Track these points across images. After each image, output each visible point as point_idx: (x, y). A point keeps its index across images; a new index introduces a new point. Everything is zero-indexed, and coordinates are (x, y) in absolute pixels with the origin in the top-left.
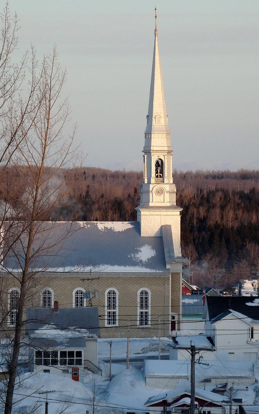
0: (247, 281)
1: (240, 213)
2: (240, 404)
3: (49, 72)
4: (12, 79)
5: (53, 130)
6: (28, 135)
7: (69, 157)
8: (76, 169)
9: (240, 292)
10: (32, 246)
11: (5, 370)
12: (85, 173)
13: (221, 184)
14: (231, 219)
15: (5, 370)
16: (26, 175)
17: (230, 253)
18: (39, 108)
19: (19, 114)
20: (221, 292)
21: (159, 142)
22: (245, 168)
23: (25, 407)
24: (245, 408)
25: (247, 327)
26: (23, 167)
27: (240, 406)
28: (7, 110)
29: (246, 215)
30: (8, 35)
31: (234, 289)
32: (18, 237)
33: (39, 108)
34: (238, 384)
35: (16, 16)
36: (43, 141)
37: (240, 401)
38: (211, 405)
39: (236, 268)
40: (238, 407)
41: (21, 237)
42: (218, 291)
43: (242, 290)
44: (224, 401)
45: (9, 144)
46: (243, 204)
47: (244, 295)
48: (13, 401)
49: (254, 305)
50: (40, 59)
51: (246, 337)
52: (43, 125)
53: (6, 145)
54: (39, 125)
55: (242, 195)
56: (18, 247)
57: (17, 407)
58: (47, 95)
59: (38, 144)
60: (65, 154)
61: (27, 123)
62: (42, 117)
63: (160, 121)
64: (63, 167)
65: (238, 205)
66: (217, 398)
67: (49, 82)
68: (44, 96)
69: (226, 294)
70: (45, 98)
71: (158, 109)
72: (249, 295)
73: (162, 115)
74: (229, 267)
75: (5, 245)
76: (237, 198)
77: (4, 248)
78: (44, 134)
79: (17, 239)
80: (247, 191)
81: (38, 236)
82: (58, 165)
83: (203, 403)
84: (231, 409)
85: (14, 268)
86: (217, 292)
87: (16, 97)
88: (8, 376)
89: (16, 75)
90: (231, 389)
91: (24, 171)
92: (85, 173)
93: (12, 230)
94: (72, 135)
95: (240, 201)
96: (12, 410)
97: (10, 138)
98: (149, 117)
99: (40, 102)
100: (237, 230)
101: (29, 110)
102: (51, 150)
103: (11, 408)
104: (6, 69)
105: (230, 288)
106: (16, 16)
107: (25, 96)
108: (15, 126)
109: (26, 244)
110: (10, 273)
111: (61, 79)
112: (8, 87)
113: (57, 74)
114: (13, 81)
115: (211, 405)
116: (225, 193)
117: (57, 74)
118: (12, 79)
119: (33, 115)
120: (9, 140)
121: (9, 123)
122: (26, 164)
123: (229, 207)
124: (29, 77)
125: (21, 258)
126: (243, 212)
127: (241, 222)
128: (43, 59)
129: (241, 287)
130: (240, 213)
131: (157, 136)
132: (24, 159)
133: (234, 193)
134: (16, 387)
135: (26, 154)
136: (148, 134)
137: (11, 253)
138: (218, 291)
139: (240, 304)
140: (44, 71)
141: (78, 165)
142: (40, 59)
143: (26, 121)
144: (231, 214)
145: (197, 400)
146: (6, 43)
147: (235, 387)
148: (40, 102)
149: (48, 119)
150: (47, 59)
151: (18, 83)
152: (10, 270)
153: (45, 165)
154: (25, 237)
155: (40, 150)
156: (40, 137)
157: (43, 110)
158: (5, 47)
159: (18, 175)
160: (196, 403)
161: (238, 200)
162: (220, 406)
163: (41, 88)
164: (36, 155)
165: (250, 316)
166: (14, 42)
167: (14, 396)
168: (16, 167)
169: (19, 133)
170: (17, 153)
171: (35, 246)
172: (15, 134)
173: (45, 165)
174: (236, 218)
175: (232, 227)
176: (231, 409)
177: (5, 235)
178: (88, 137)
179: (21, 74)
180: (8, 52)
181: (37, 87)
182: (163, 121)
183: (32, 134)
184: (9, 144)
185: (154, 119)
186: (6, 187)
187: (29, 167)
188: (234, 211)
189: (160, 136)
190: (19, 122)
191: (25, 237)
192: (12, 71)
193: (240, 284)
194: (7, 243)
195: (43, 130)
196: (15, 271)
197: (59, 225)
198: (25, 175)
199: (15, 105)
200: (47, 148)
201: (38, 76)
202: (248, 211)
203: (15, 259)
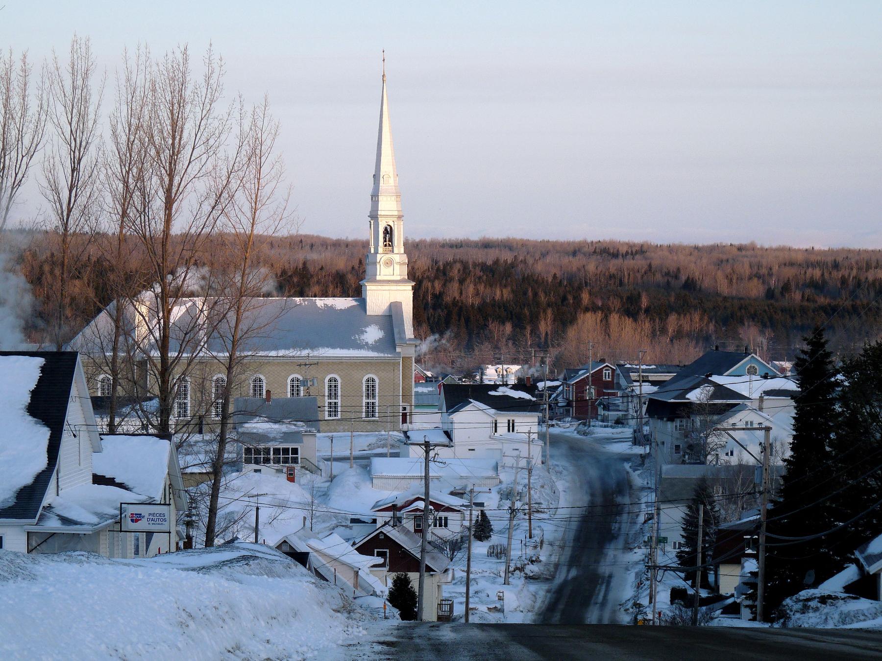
0: (490, 366)
1: (481, 288)
2: (482, 508)
3: (259, 124)
4: (217, 132)
5: (265, 192)
6: (235, 198)
7: (283, 222)
8: (291, 237)
9: (481, 379)
10: (240, 327)
11: (209, 469)
12: (301, 241)
13: (460, 253)
14: (471, 294)
15: (209, 470)
16: (233, 244)
17: (470, 334)
18: (248, 166)
19: (225, 173)
20: (460, 379)
21: (388, 206)
22: (487, 236)
23: (232, 513)
24: (488, 513)
25: (489, 420)
26: (229, 234)
27: (482, 511)
28: (211, 168)
29: (488, 290)
30: (211, 81)
31: (475, 376)
32: (224, 316)
33: (248, 166)
34: (480, 486)
35: (221, 60)
36: (253, 205)
37: (481, 505)
38: (449, 509)
39: (477, 352)
40: (479, 512)
41: (228, 316)
42: (456, 377)
43: (484, 377)
44: (463, 506)
45: (213, 208)
46: (485, 277)
47: (487, 382)
48: (219, 506)
49: (520, 392)
50: (248, 109)
51: (489, 431)
52: (253, 186)
53: (210, 209)
54: (248, 185)
55: (484, 267)
56: (224, 327)
57: (223, 512)
58: (258, 151)
59: (247, 208)
60: (278, 219)
61: (234, 185)
62: (252, 176)
63: (388, 182)
64: (276, 235)
65: (480, 278)
66: (455, 502)
67: (259, 135)
68: (254, 153)
69: (466, 382)
70: (255, 155)
71: (387, 167)
72: (492, 383)
73: (391, 175)
74: (469, 348)
75: (208, 324)
76: (478, 270)
77: (207, 328)
78: (254, 196)
79: (223, 319)
80: (489, 262)
81: (246, 314)
82: (270, 232)
83: (438, 507)
84: (471, 514)
85: (219, 352)
86: (455, 379)
87: (221, 154)
88: (212, 477)
89: (221, 128)
90: (471, 491)
91: (231, 239)
92: (301, 241)
93: (217, 308)
94: (286, 197)
95: (481, 274)
96: (217, 516)
97: (214, 201)
98: (376, 177)
99: (249, 159)
100: (479, 308)
101: (236, 168)
102: (263, 214)
103: (215, 514)
104: (210, 121)
105: (469, 375)
106: (221, 60)
107: (232, 154)
108: (220, 186)
109: (233, 324)
110: (215, 357)
111: (273, 132)
112: (211, 142)
113: (269, 127)
114: (217, 135)
115: (449, 509)
116: (465, 266)
117: (269, 127)
118: (217, 132)
119: (241, 174)
120: (213, 204)
121: (212, 183)
122: (233, 231)
123: (468, 281)
124: (236, 130)
125: (227, 340)
126: (485, 287)
127: (483, 299)
128: (253, 109)
129: (482, 374)
130: (481, 288)
131: (385, 198)
132: (230, 225)
133: (475, 265)
134: (222, 489)
135: (233, 219)
136: (375, 197)
137: (215, 334)
138: (456, 377)
139: (482, 393)
140: (254, 123)
141: (293, 232)
142: (248, 109)
143: (233, 181)
144: (471, 289)
145: (432, 503)
146: (209, 90)
147: (476, 489)
148: (249, 159)
149: (259, 179)
150: (257, 110)
151: (223, 137)
152: (215, 354)
153: (255, 232)
154: (232, 316)
155: (249, 215)
156: (249, 198)
157: (253, 168)
158: (209, 96)
159: (223, 244)
160: (431, 507)
161: (479, 273)
162: (459, 511)
163: (251, 143)
164: (244, 221)
165: (493, 406)
166: (218, 89)
167: (220, 500)
168: (221, 235)
169: (225, 195)
170: (222, 219)
171: (243, 326)
172: (220, 195)
173: (255, 232)
174: (477, 294)
175: (473, 303)
176: (471, 514)
177: (209, 314)
178: (306, 204)
179: (227, 127)
180: (212, 101)
181: (246, 142)
182: (392, 181)
183: (241, 198)
184: (213, 208)
185: (381, 179)
186: (209, 257)
187: (237, 235)
188: (475, 285)
189: (389, 198)
190: (225, 182)
191: (232, 316)
192: (216, 123)
193: (482, 369)
194: (210, 323)
195: (253, 191)
196: (221, 355)
197: (272, 301)
198: (231, 243)
199: (220, 162)
200: (258, 212)
201: (246, 128)
202: (491, 286)
203: (220, 341)
